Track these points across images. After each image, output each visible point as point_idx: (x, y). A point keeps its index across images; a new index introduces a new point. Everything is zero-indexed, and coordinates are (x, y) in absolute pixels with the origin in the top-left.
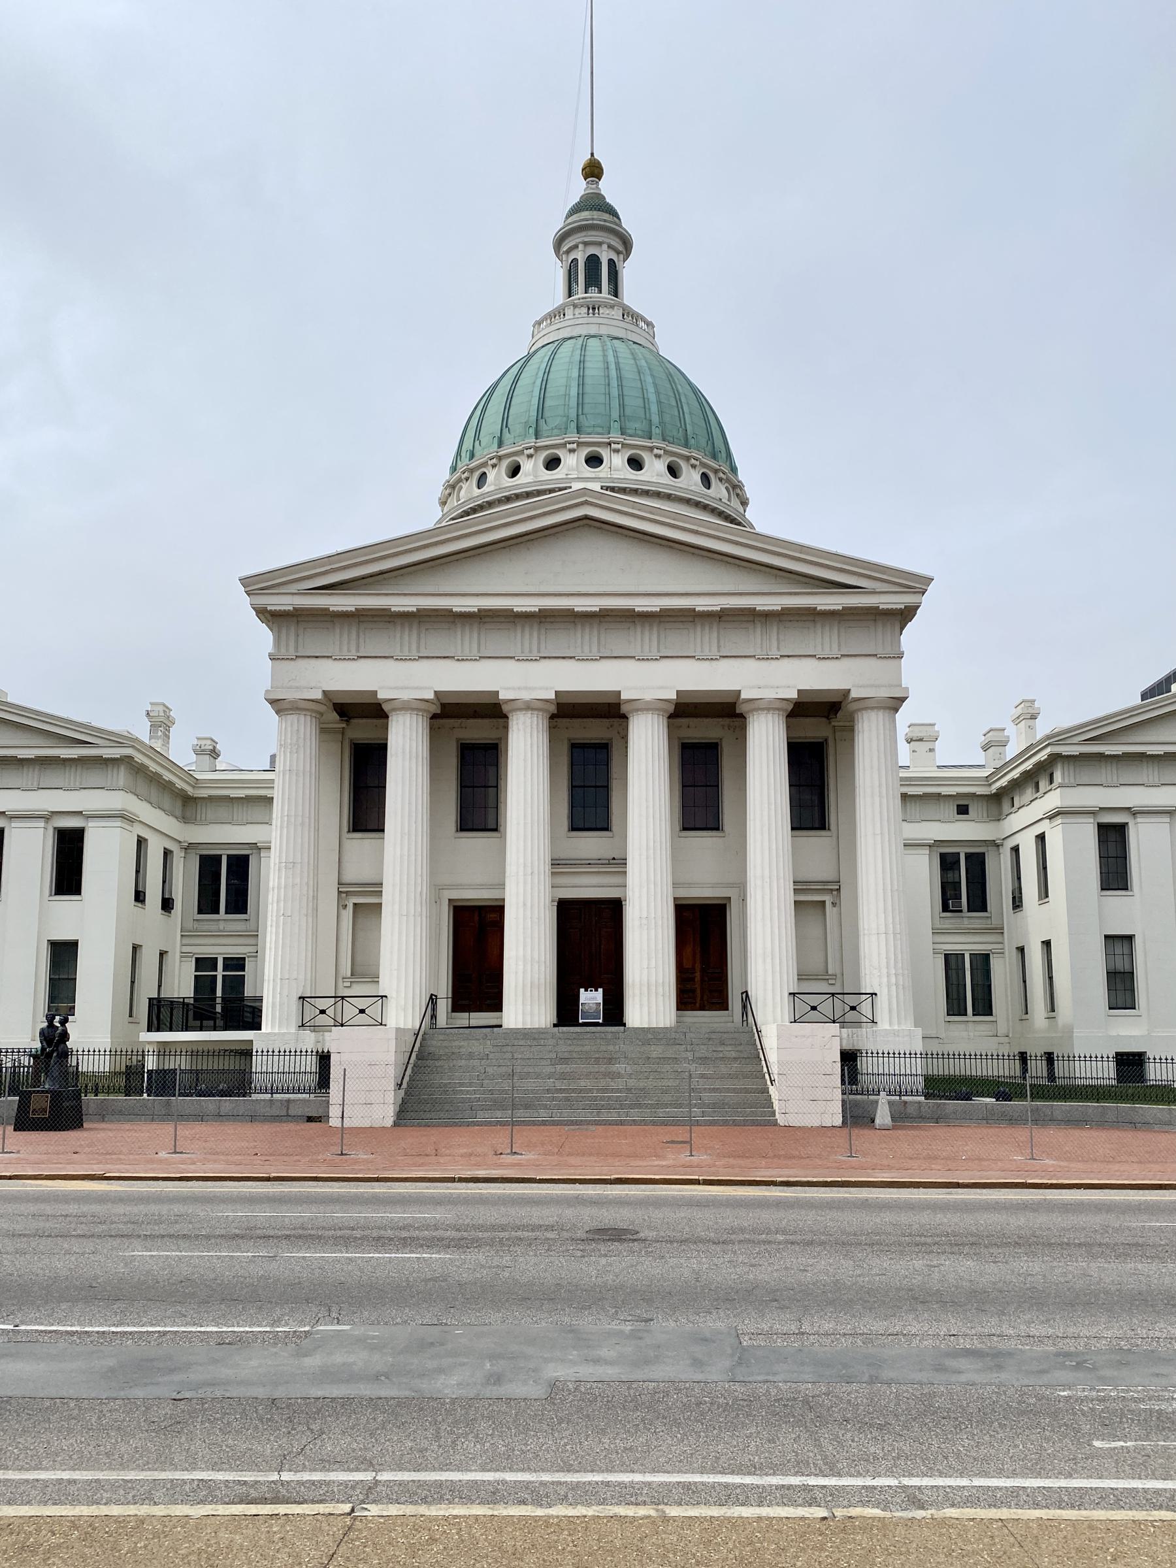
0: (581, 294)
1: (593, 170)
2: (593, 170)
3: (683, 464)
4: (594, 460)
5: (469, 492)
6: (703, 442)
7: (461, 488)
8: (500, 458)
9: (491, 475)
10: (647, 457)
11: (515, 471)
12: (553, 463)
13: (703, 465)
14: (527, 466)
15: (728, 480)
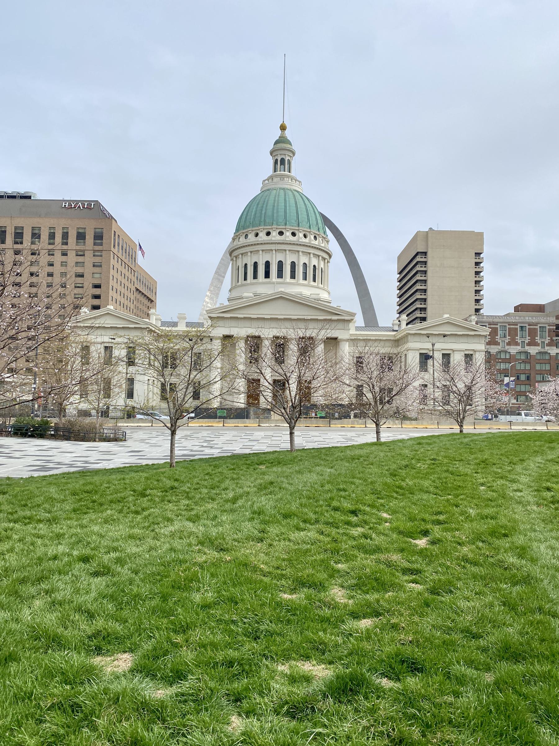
0: (279, 172)
1: (283, 128)
2: (283, 128)
3: (308, 234)
4: (281, 233)
5: (242, 240)
6: (315, 226)
7: (239, 238)
8: (252, 230)
9: (250, 236)
10: (296, 232)
11: (257, 235)
12: (268, 234)
13: (314, 233)
14: (261, 234)
15: (323, 237)
